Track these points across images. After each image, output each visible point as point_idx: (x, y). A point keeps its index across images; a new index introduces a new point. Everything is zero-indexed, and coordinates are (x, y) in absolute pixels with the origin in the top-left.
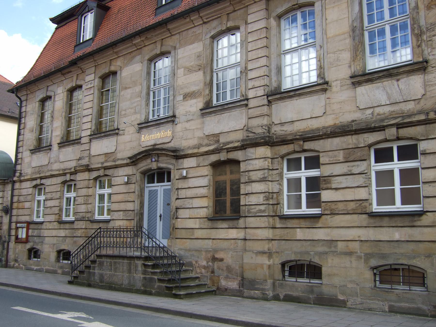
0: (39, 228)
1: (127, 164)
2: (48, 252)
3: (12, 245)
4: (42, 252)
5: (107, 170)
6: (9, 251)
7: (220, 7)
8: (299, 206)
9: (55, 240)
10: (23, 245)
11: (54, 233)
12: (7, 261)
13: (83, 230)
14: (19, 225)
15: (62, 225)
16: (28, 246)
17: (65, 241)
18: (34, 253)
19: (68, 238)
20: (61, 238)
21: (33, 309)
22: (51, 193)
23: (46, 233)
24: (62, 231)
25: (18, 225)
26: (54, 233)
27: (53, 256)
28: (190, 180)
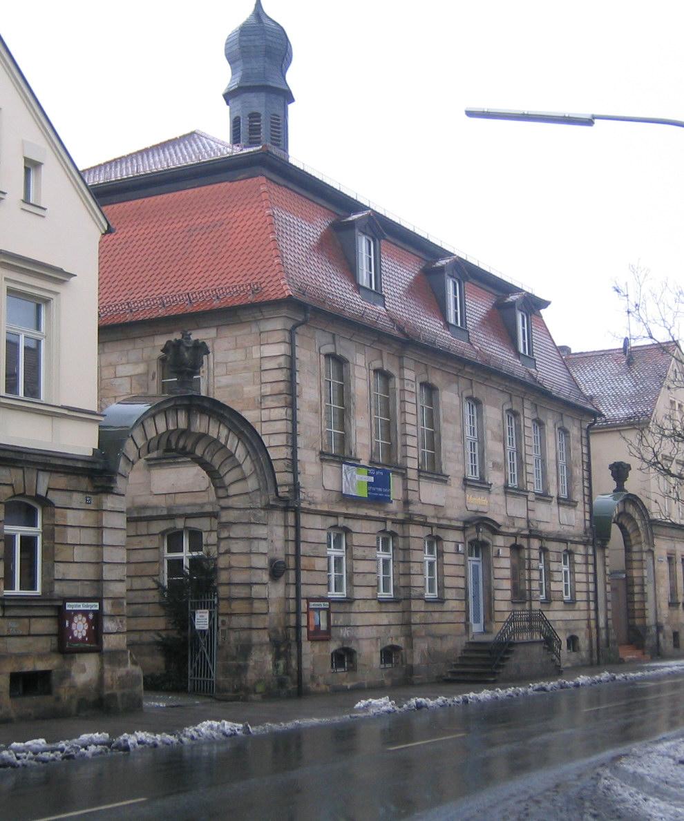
0: (347, 610)
1: (459, 527)
2: (369, 653)
3: (307, 646)
4: (360, 655)
5: (442, 531)
6: (303, 659)
7: (46, 273)
8: (12, 588)
9: (373, 632)
10: (324, 645)
11: (372, 619)
12: (299, 681)
13: (422, 614)
14: (312, 605)
15: (383, 606)
16: (334, 646)
17: (390, 631)
18: (345, 657)
19: (392, 627)
20: (383, 627)
21: (58, 814)
22: (363, 549)
23: (358, 619)
24: (384, 615)
25: (311, 604)
26: (372, 619)
27: (376, 658)
28: (501, 559)
